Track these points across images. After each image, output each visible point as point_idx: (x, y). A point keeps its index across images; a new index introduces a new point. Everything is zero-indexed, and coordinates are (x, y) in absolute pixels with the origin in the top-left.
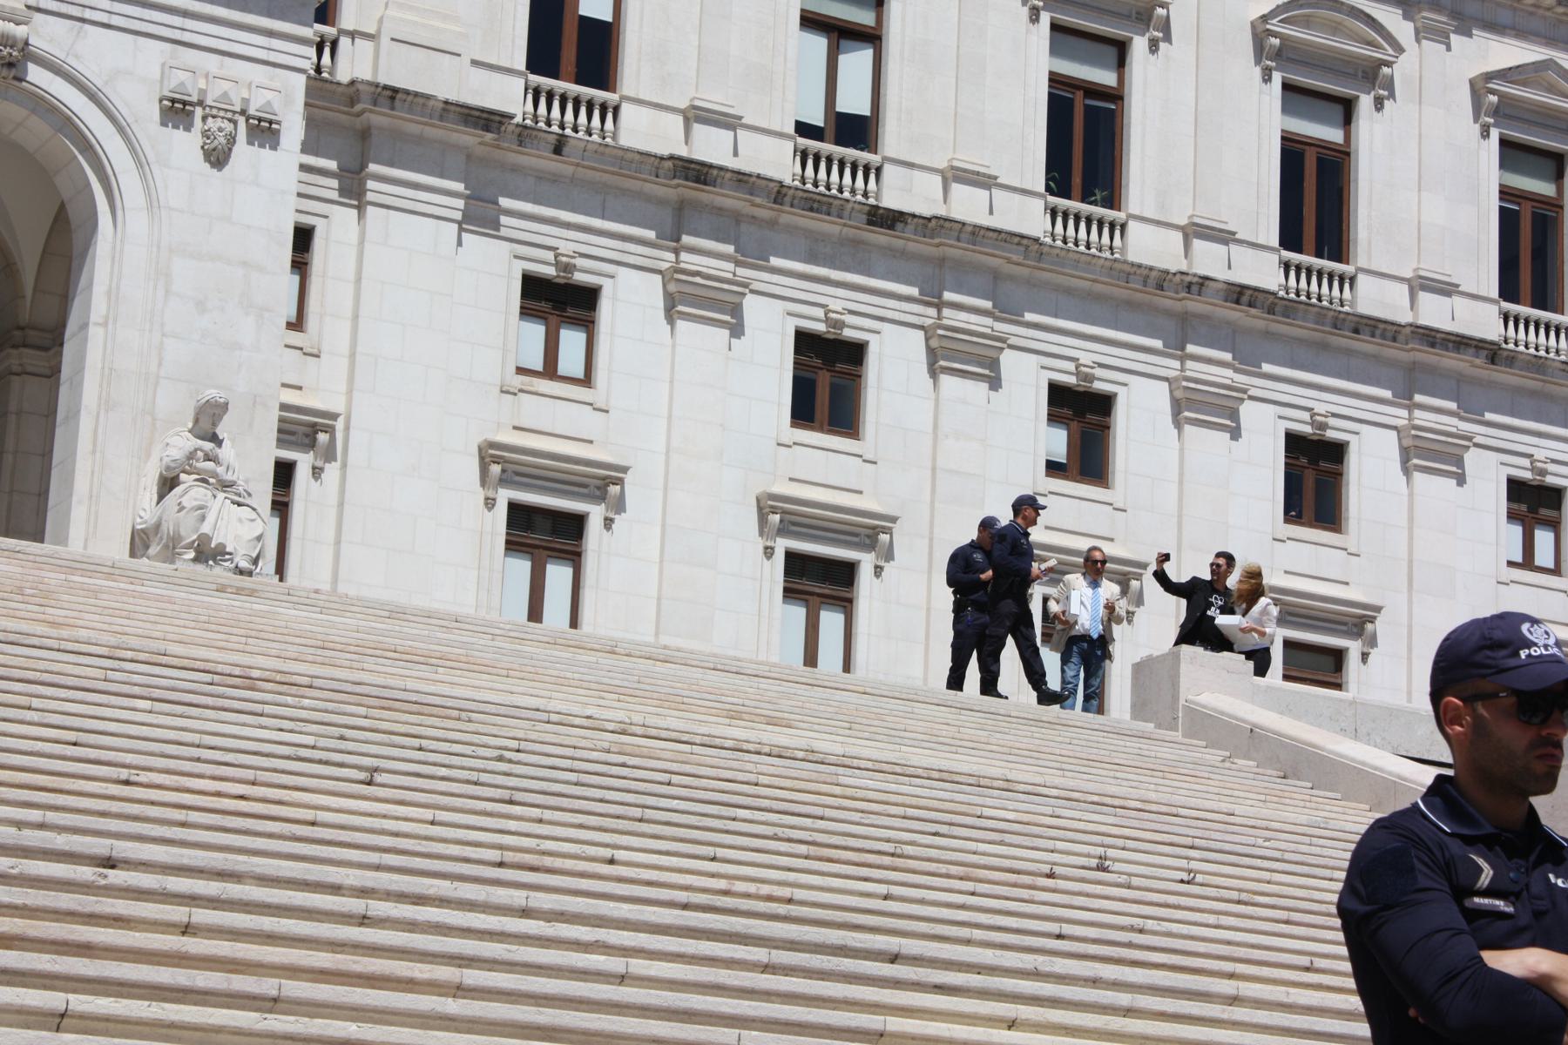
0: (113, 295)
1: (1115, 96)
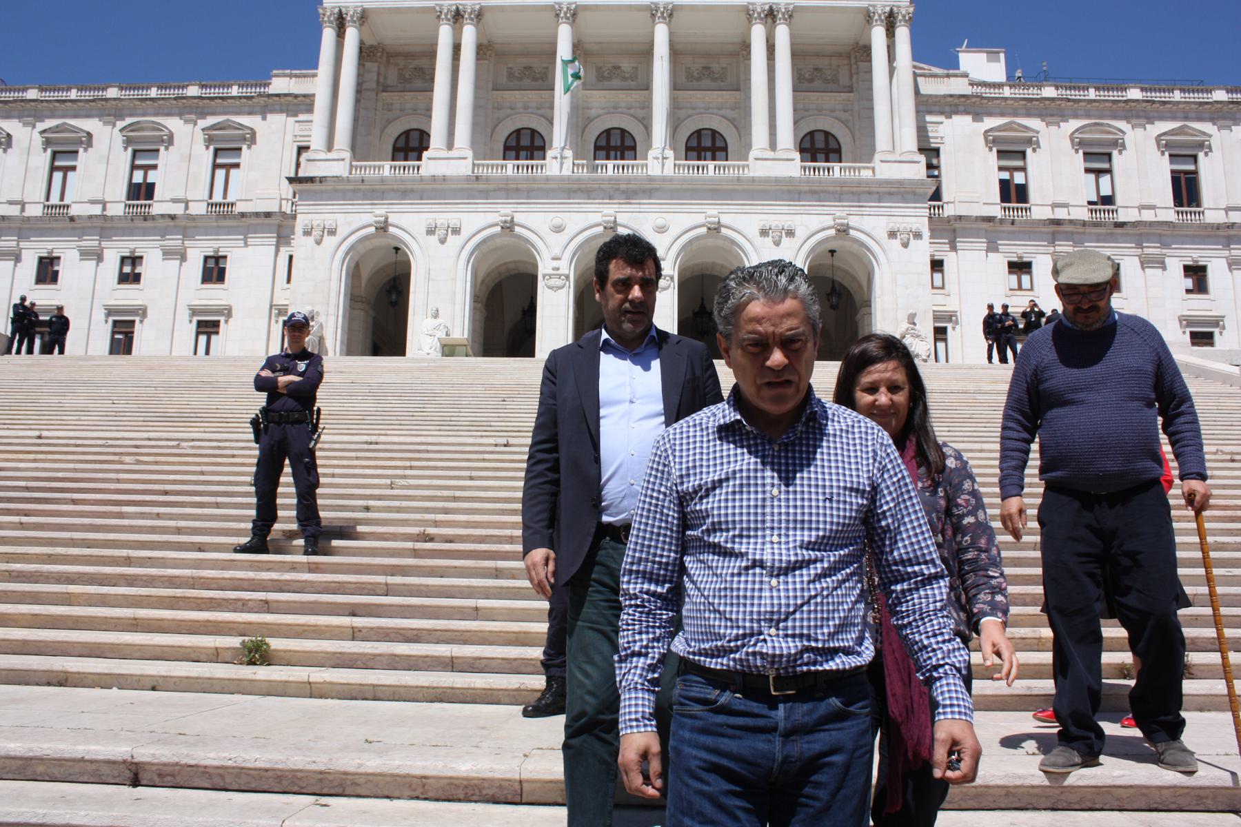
1: (1195, 172)
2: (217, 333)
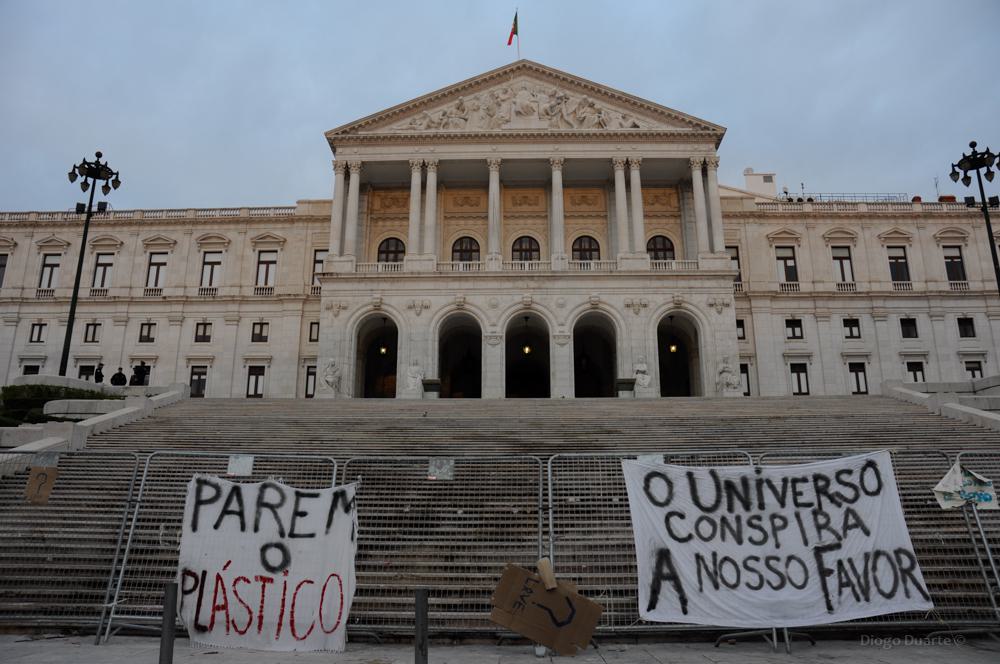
0: (705, 342)
2: (263, 374)
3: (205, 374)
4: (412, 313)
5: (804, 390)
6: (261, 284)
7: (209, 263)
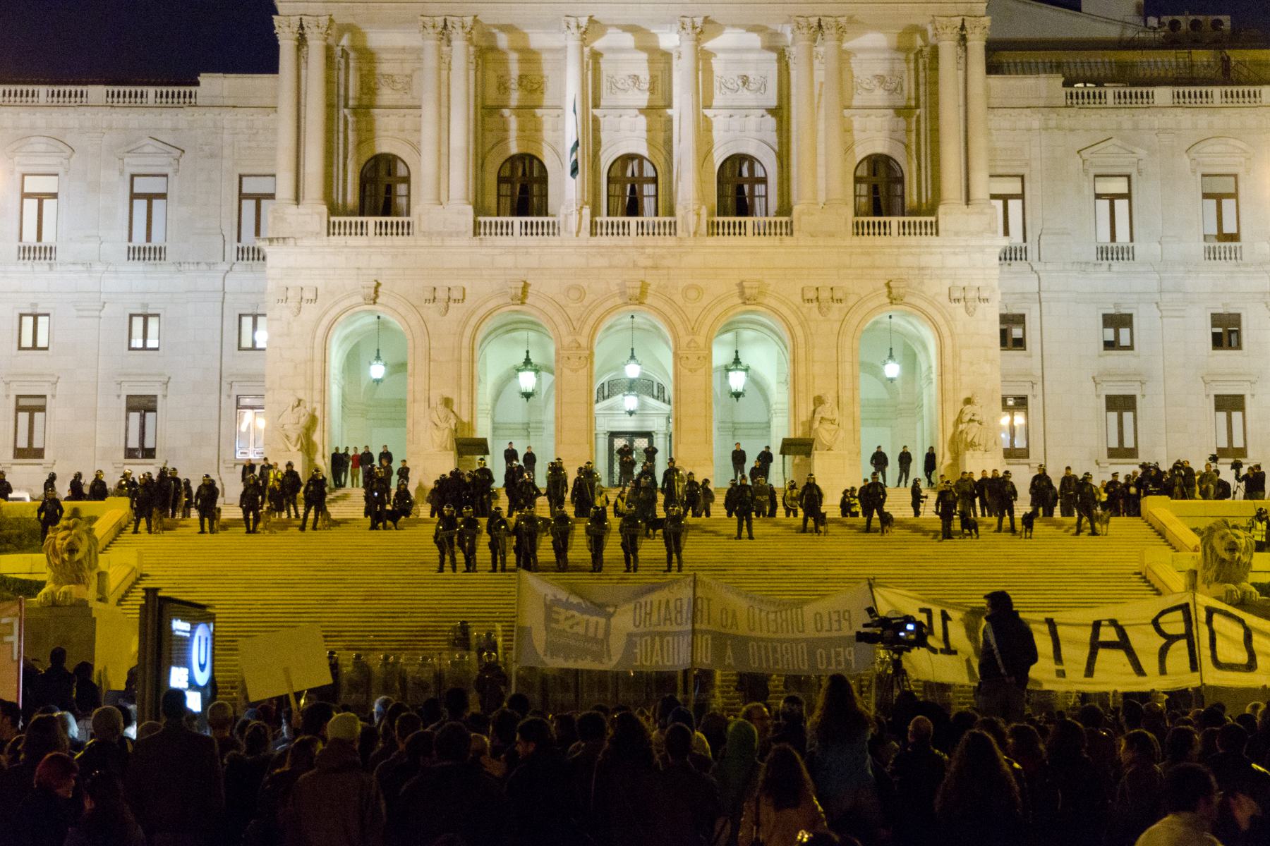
2: (154, 410)
3: (42, 409)
4: (431, 311)
5: (1129, 443)
6: (139, 239)
7: (30, 195)
